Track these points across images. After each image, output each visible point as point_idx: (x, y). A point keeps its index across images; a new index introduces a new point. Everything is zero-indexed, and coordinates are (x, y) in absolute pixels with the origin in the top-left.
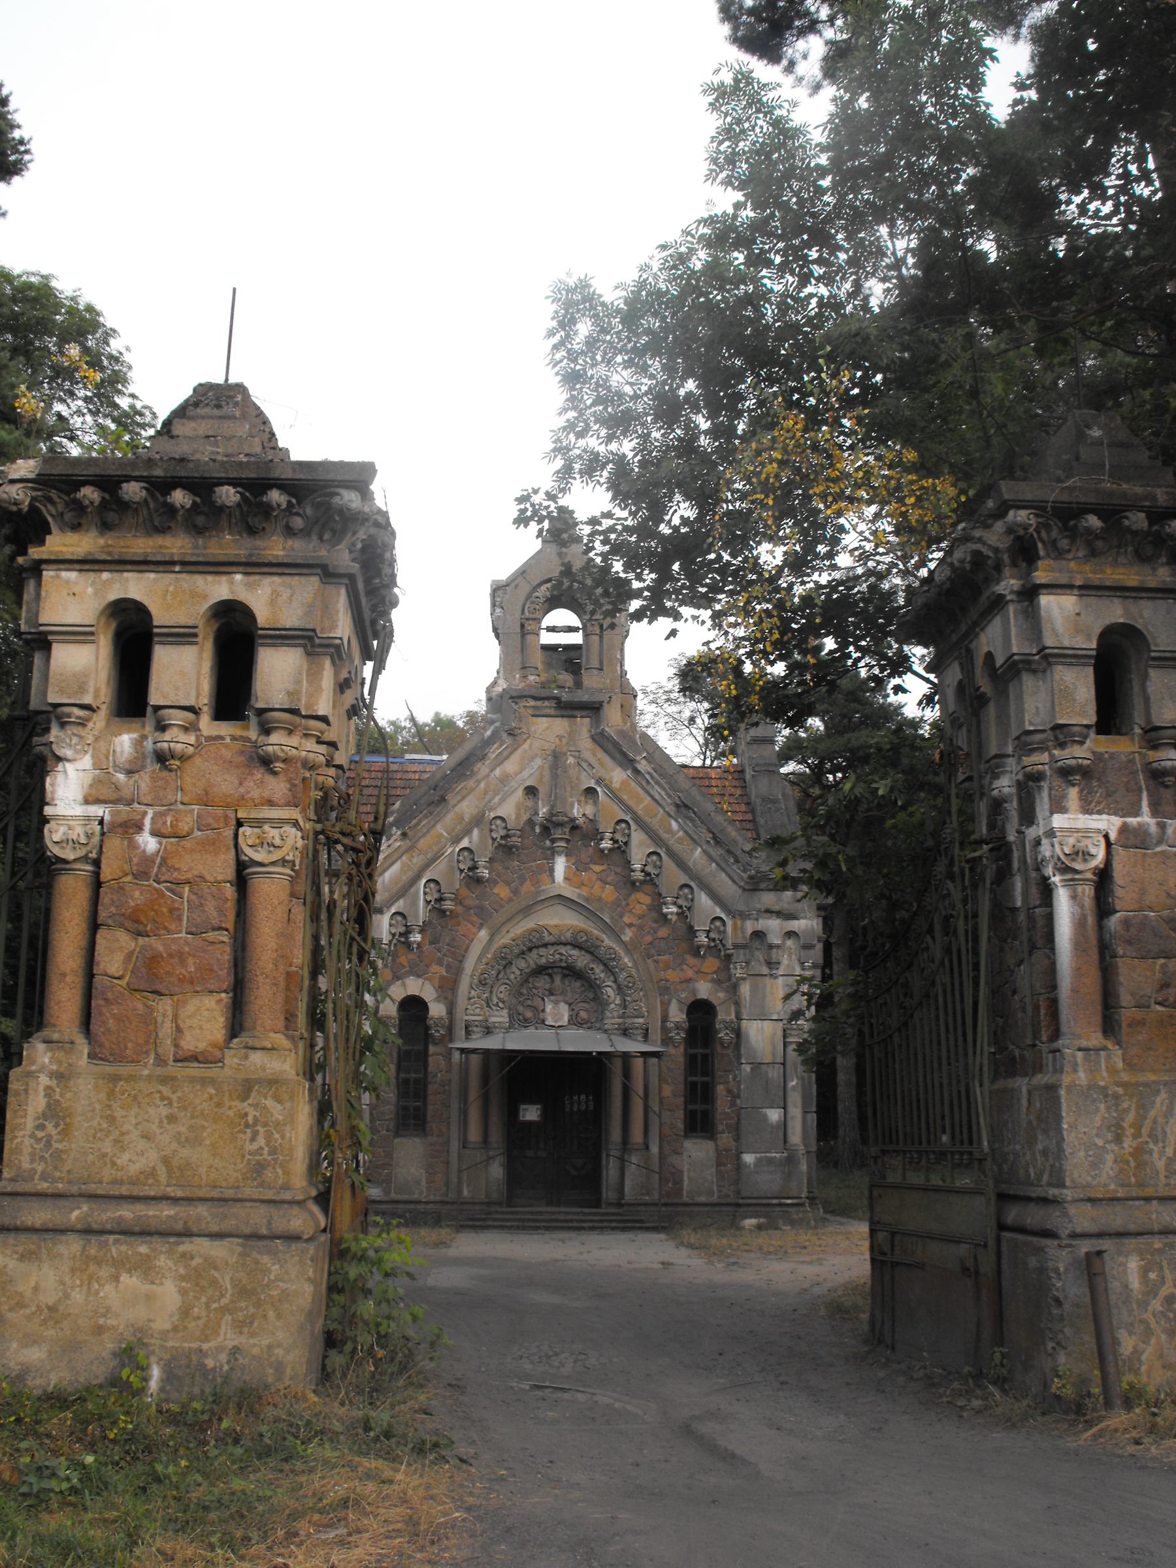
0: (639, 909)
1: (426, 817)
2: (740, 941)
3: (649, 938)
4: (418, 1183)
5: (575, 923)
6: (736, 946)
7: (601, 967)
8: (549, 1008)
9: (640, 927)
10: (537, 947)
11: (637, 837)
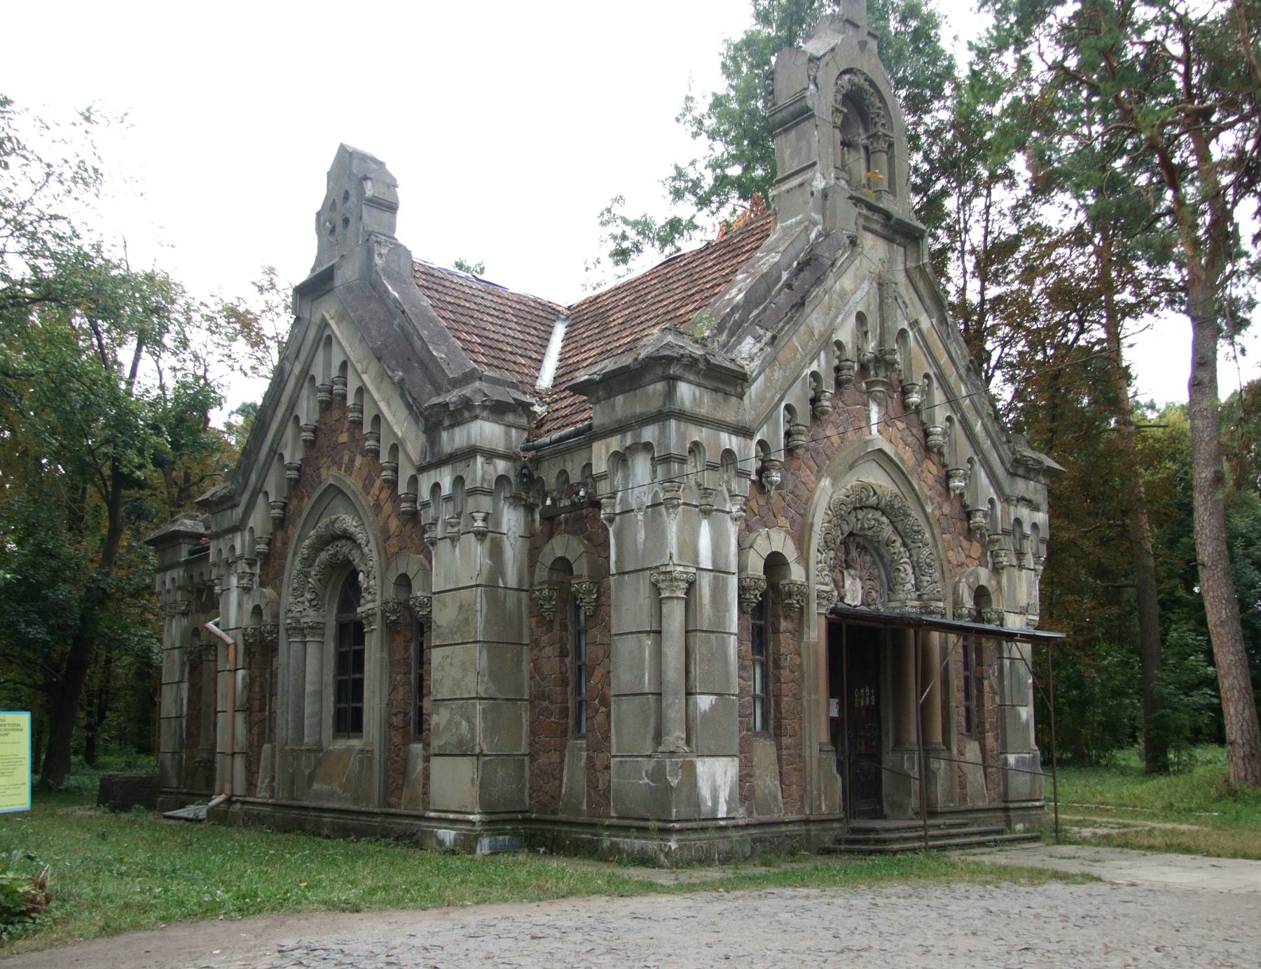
1: (788, 322)
2: (1008, 527)
4: (775, 798)
5: (885, 484)
6: (1005, 532)
8: (848, 583)
11: (938, 396)
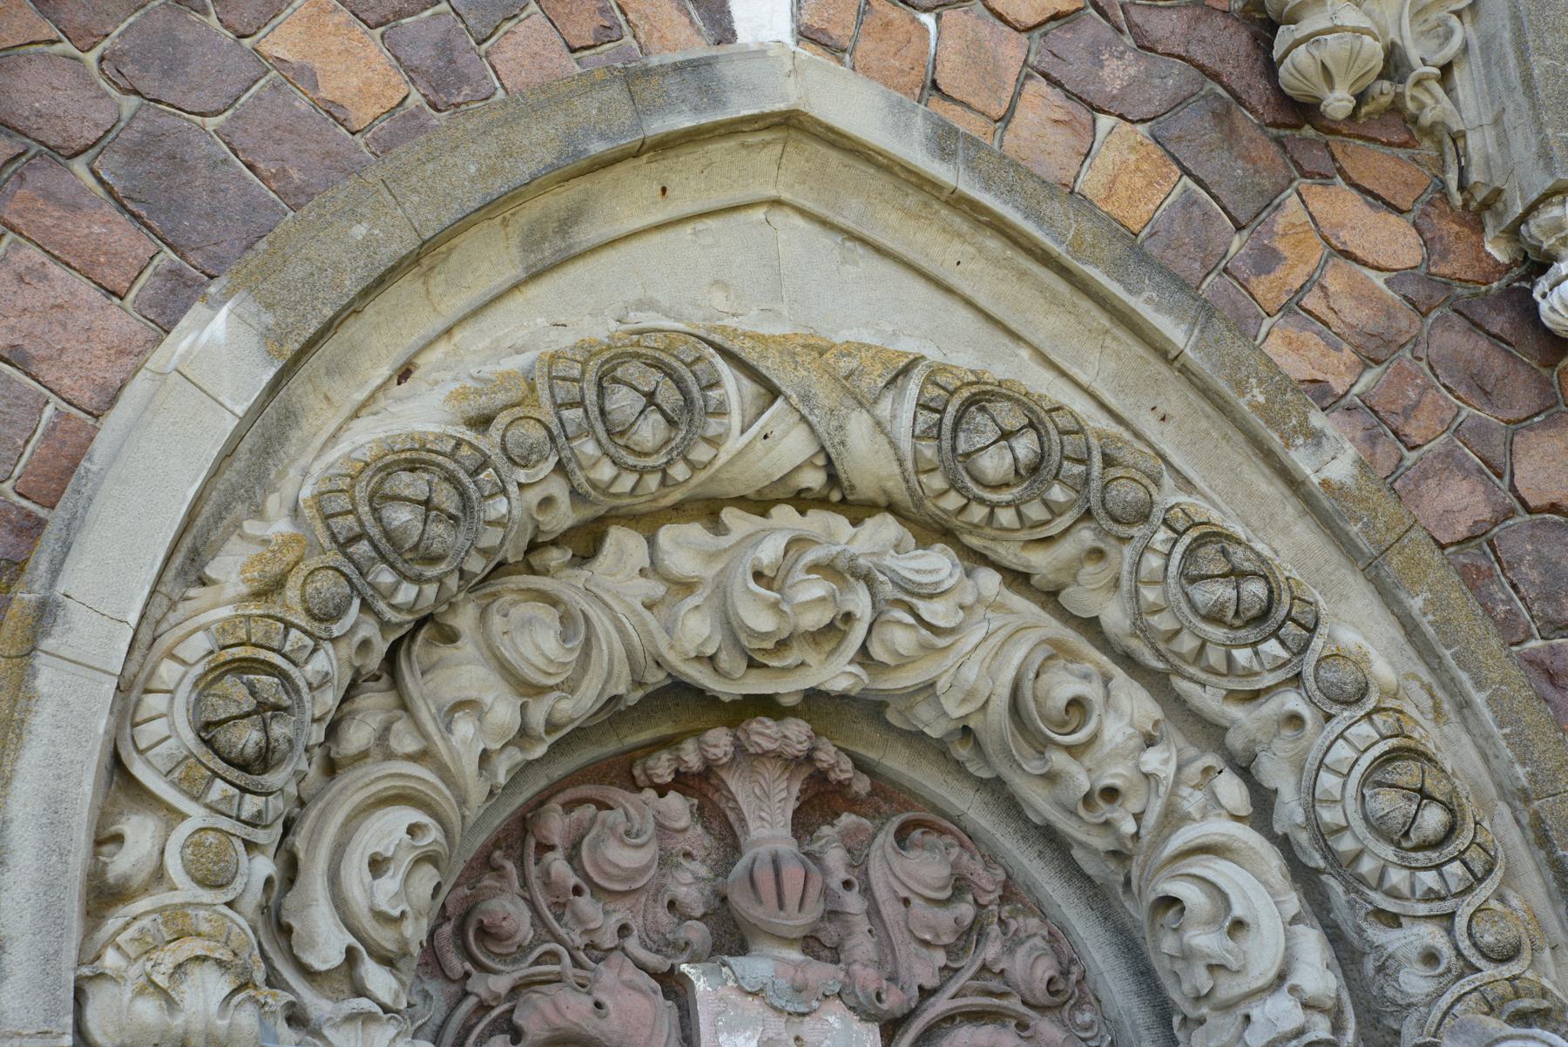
0: (1350, 299)
3: (1461, 501)
7: (1134, 705)
9: (1380, 422)
10: (647, 521)
